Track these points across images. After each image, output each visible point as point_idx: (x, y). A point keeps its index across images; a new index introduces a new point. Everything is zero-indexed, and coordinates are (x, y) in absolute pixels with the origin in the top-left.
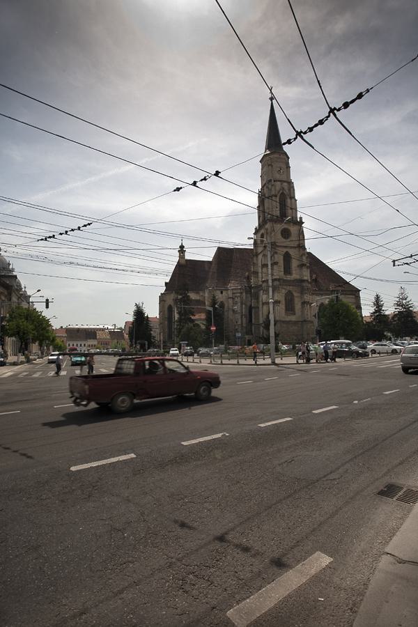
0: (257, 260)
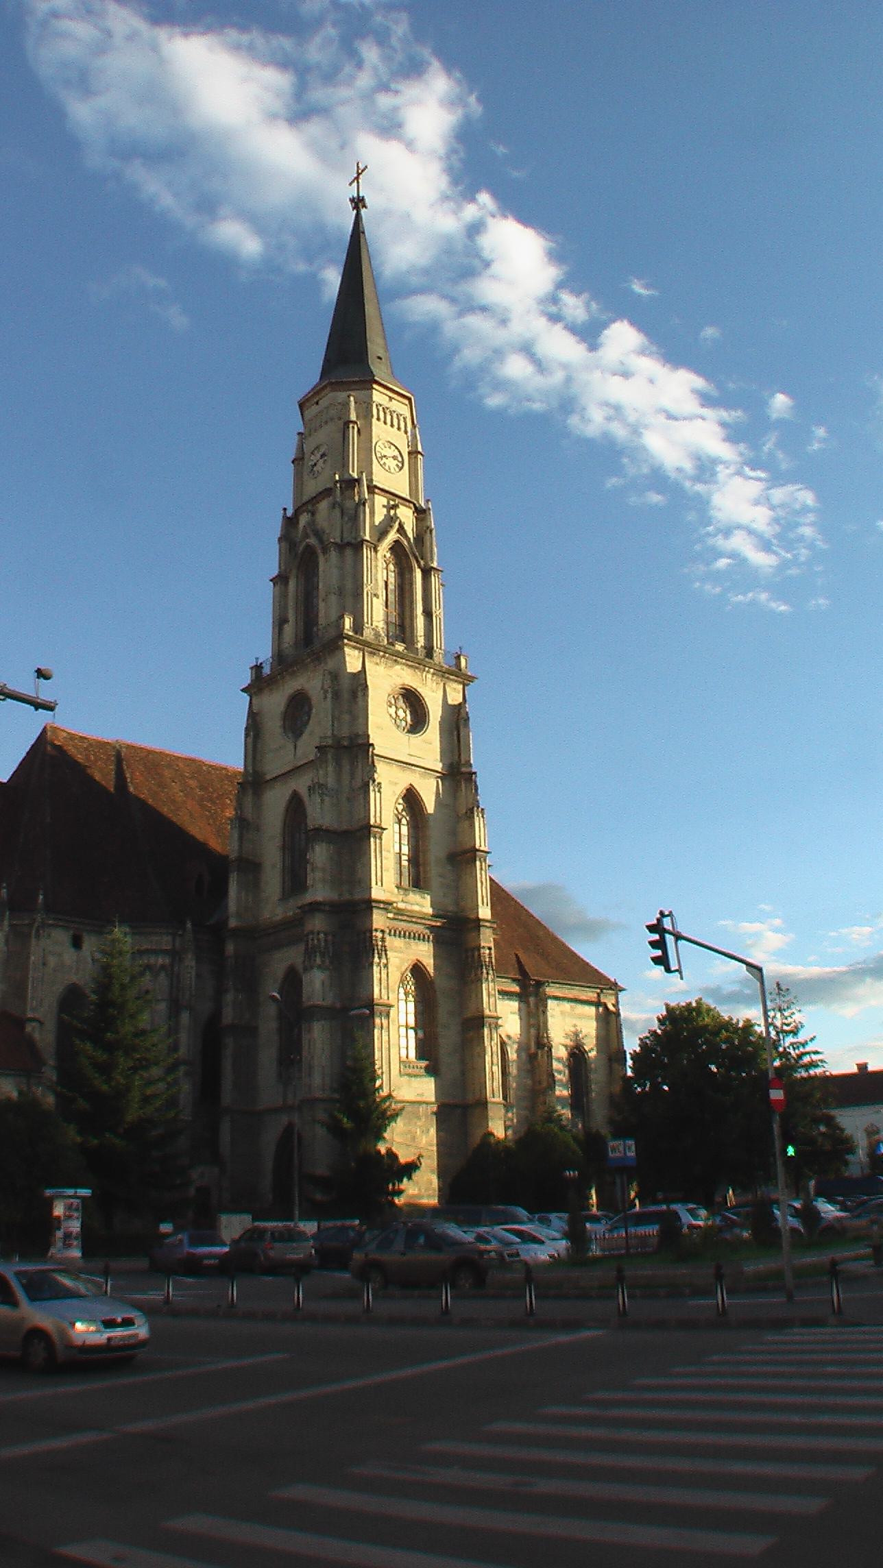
0: (258, 806)
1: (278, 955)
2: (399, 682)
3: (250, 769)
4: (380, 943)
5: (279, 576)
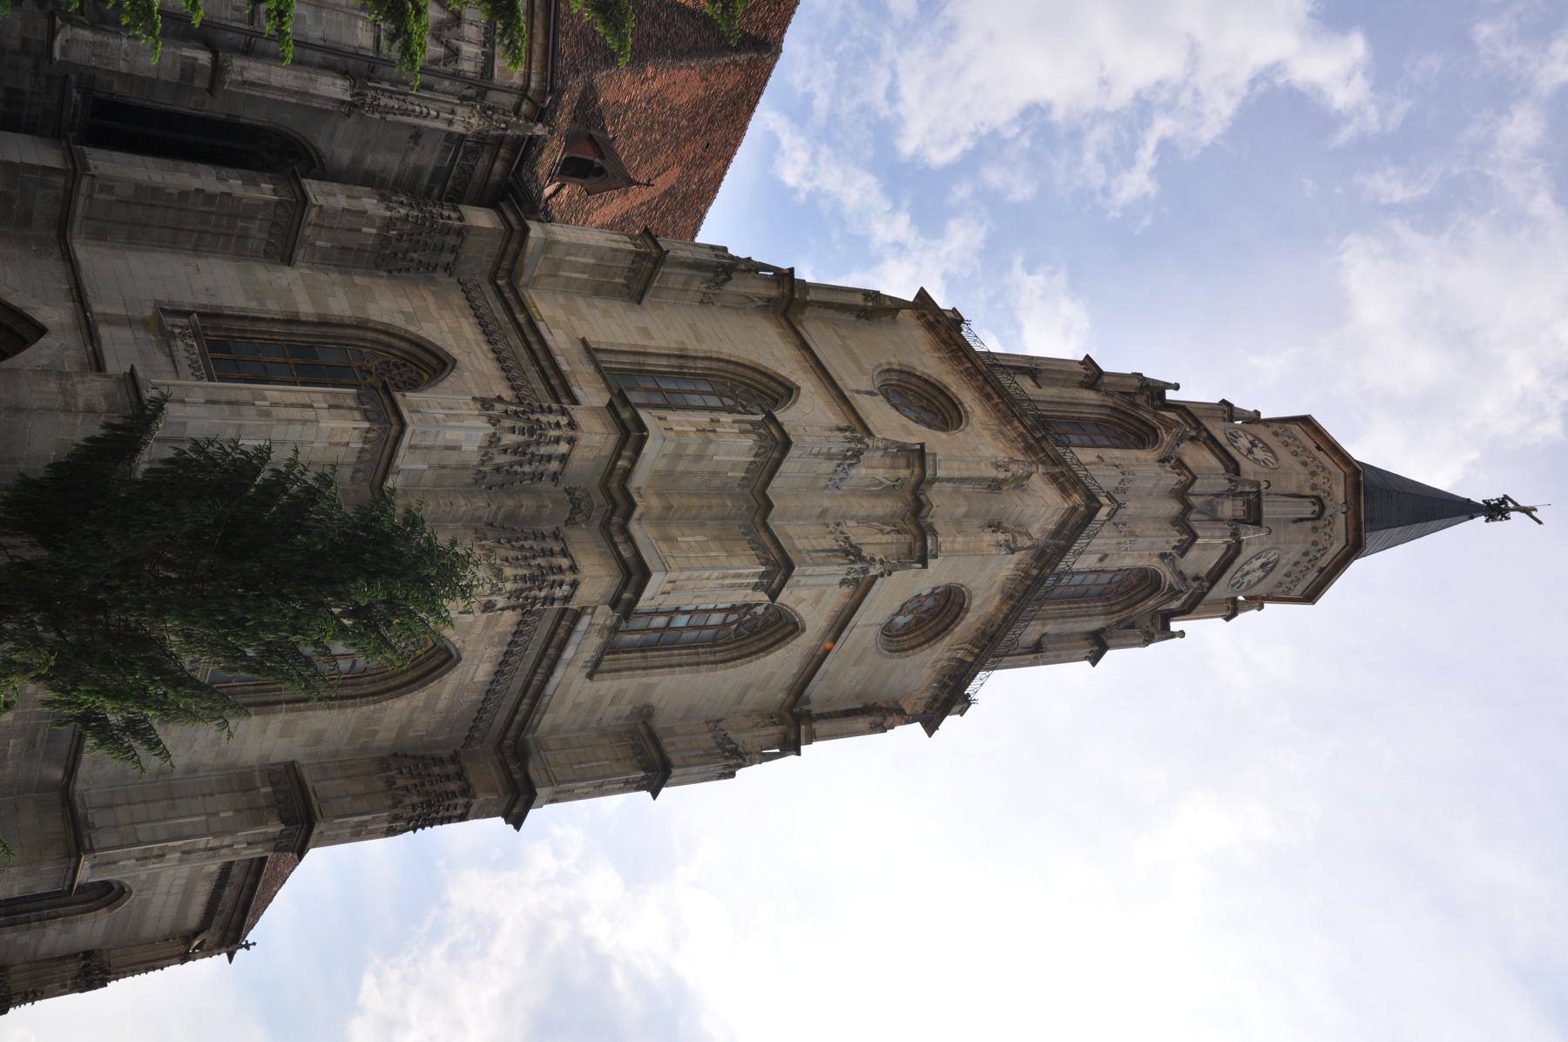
0: (745, 304)
1: (469, 328)
2: (975, 603)
3: (811, 296)
5: (1100, 372)
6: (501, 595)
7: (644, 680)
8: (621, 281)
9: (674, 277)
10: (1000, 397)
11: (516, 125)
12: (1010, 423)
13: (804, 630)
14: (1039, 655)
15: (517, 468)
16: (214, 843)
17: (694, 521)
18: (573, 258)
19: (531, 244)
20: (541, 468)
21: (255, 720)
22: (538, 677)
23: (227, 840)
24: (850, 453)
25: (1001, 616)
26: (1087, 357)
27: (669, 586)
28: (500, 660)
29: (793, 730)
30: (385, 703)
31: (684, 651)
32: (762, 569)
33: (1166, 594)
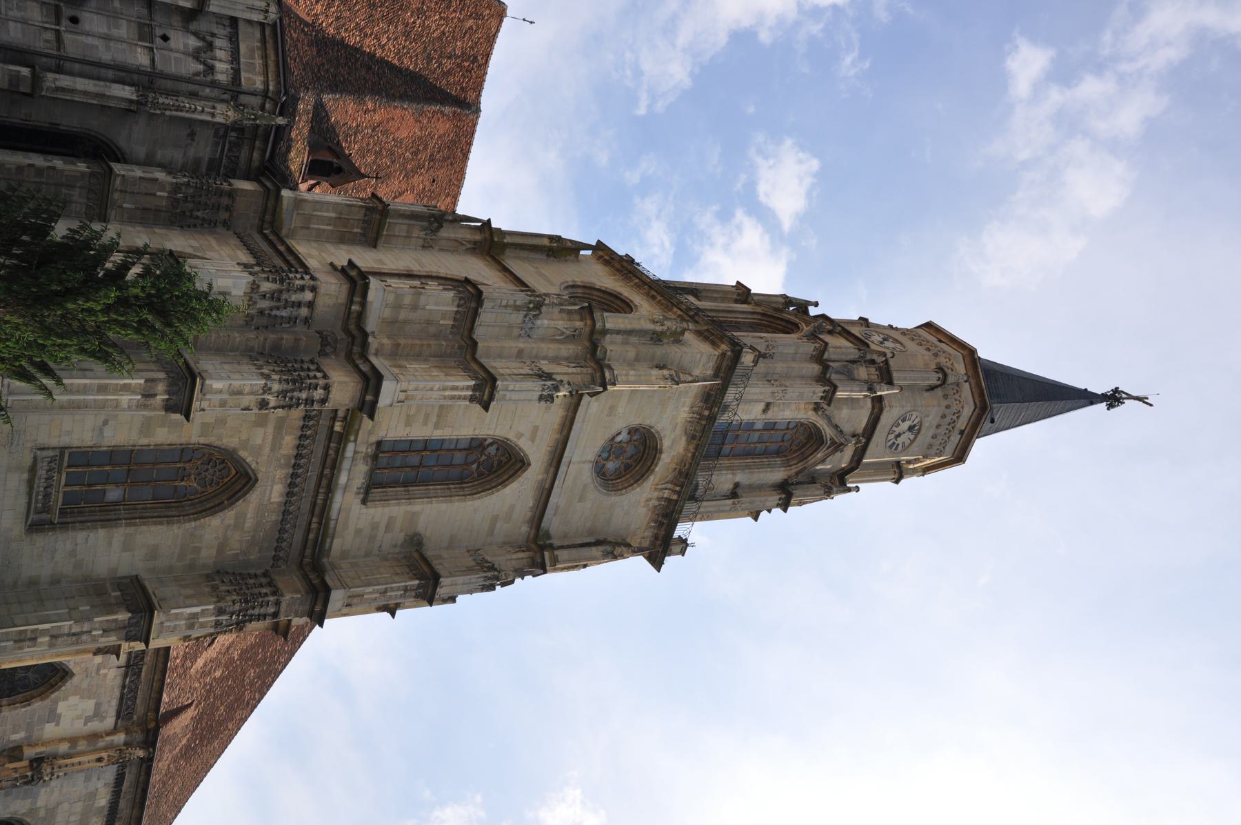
0: (457, 247)
2: (666, 443)
3: (508, 240)
4: (304, 395)
6: (271, 394)
7: (409, 508)
8: (359, 230)
9: (400, 227)
10: (662, 296)
11: (262, 117)
12: (671, 310)
13: (529, 465)
14: (736, 500)
15: (274, 312)
16: (76, 629)
17: (418, 356)
18: (319, 213)
19: (285, 202)
20: (295, 313)
21: (102, 533)
22: (321, 497)
23: (86, 627)
24: (531, 306)
25: (690, 455)
26: (738, 282)
27: (402, 396)
28: (288, 482)
29: (538, 555)
30: (202, 520)
31: (438, 487)
32: (473, 383)
33: (829, 447)
